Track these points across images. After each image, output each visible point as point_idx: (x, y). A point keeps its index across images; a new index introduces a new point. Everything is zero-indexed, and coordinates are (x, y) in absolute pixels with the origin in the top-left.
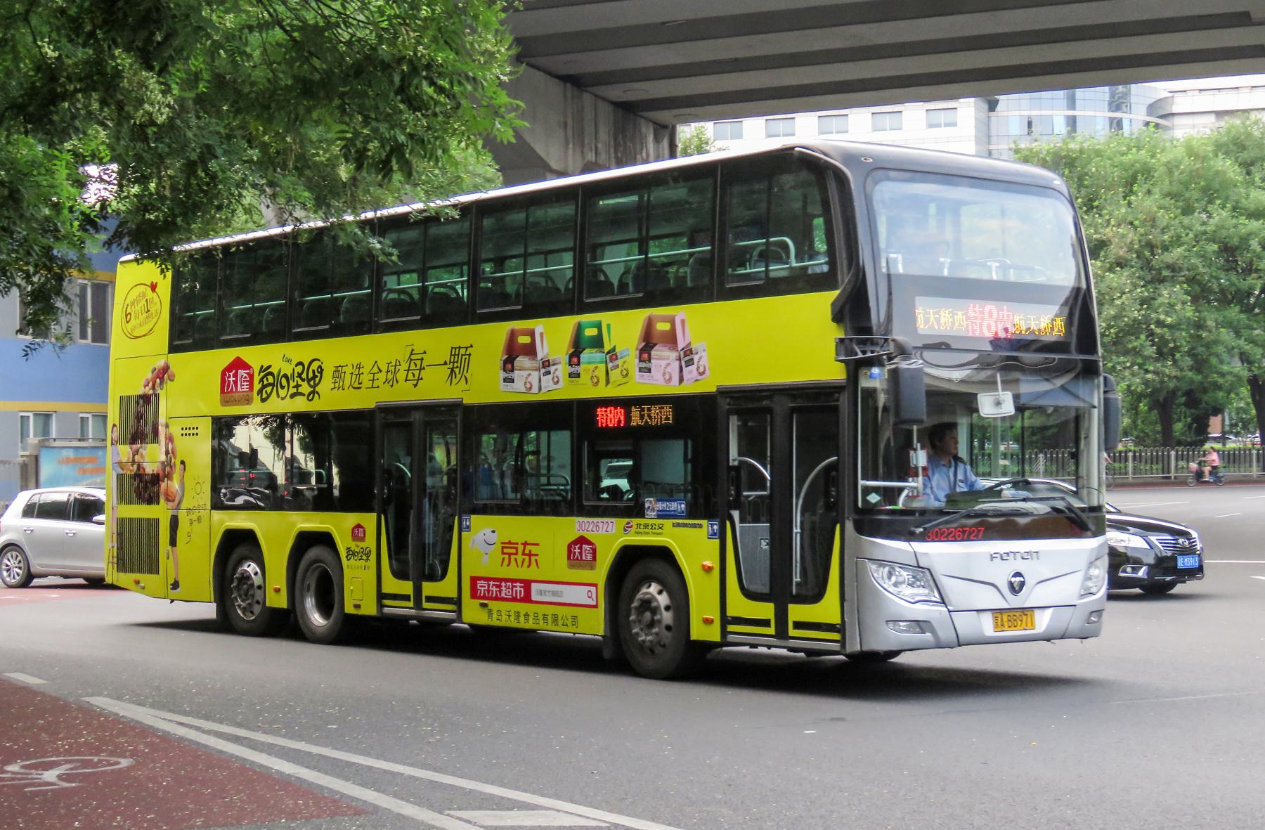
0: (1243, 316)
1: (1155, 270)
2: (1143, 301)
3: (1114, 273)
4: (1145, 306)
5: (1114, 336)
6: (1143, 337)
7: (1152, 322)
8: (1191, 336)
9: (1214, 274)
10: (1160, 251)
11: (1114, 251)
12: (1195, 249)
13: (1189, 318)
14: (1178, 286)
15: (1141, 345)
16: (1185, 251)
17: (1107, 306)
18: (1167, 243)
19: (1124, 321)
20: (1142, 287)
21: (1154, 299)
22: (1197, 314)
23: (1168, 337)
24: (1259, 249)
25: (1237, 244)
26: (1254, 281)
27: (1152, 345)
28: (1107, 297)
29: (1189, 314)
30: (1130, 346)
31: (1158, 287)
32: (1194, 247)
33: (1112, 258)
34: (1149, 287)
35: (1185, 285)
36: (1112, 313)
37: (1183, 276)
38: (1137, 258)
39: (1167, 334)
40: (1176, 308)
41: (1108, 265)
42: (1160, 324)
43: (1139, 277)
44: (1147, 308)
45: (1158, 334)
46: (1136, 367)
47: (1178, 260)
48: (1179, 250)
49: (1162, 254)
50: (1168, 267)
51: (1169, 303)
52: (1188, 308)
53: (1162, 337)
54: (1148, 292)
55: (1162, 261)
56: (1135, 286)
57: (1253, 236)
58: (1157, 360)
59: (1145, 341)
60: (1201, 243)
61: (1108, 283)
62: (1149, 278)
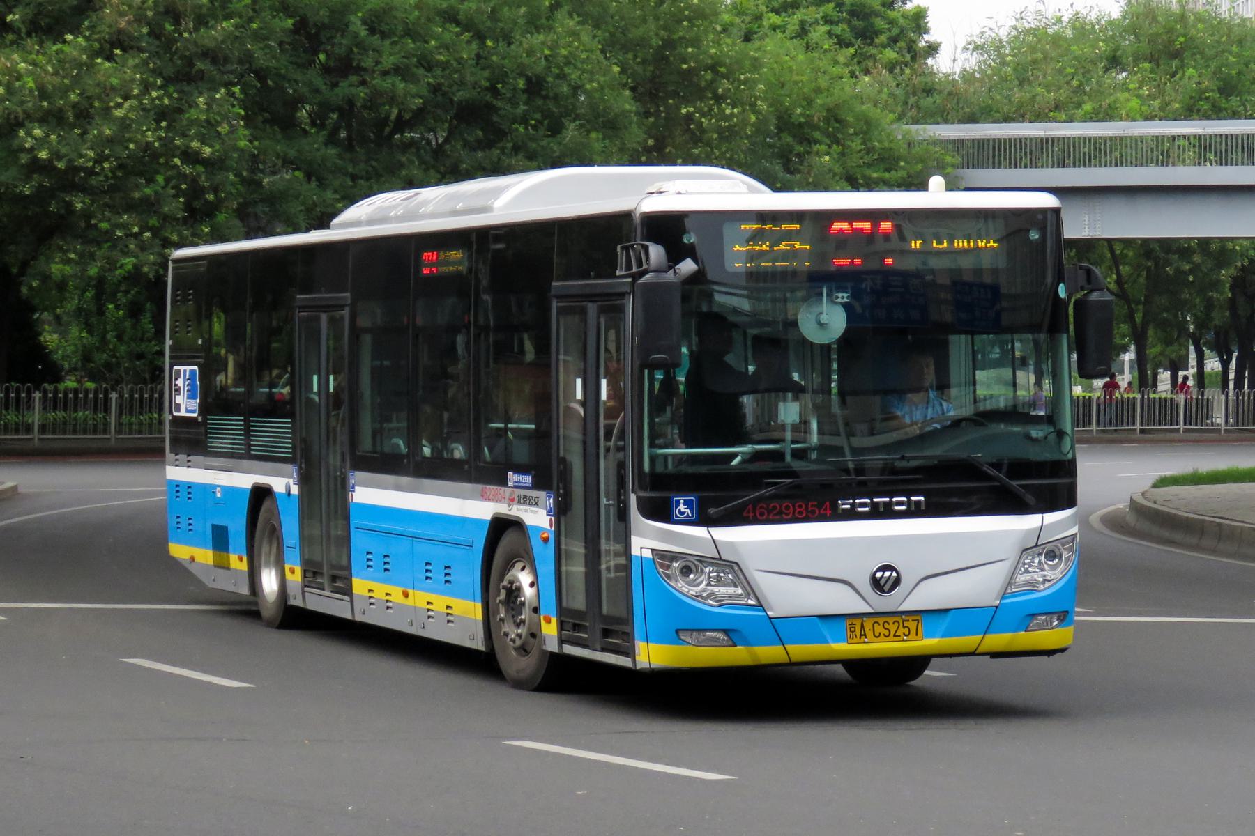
0: (332, 151)
1: (182, 57)
2: (162, 114)
3: (110, 58)
4: (164, 124)
5: (110, 174)
6: (160, 179)
7: (178, 152)
8: (243, 181)
9: (283, 71)
10: (191, 25)
11: (108, 20)
12: (255, 26)
13: (242, 151)
14: (223, 90)
15: (156, 193)
16: (237, 27)
17: (98, 120)
18: (204, 11)
19: (127, 148)
20: (160, 88)
21: (180, 111)
22: (256, 143)
23: (204, 182)
24: (363, 33)
25: (326, 20)
26: (354, 90)
27: (176, 196)
28: (97, 104)
29: (242, 144)
30: (137, 195)
31: (186, 88)
32: (251, 20)
33: (105, 31)
34: (171, 89)
35: (237, 89)
36: (108, 132)
37: (232, 72)
38: (149, 34)
39: (203, 178)
40: (219, 129)
41: (97, 45)
42: (191, 157)
43: (153, 71)
44: (168, 128)
45: (185, 176)
46: (148, 234)
47: (223, 42)
48: (225, 24)
49: (196, 29)
50: (207, 54)
51: (208, 121)
52: (243, 132)
53: (194, 181)
54: (170, 97)
55: (195, 42)
56: (146, 87)
57: (353, 7)
58: (185, 221)
59: (163, 188)
60: (263, 14)
61: (100, 77)
62: (169, 71)
